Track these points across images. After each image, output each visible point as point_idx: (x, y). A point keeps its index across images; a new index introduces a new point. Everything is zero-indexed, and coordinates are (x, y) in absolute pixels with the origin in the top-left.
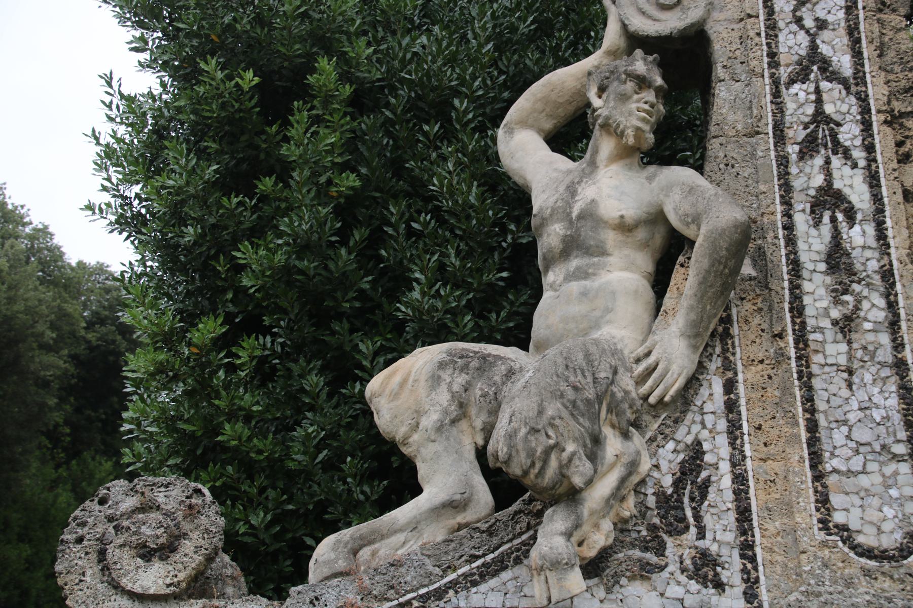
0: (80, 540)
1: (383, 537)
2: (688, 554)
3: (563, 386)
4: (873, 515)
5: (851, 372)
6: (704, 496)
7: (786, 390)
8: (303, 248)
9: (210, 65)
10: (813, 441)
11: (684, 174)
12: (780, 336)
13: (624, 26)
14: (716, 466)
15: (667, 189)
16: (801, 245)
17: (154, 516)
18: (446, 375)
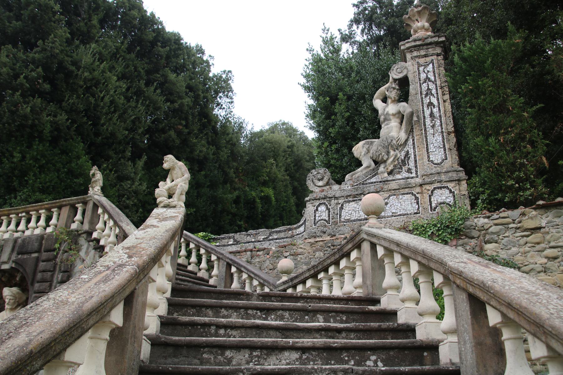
3: (382, 144)
4: (437, 158)
7: (423, 139)
8: (341, 127)
9: (321, 98)
10: (427, 147)
11: (404, 104)
12: (422, 130)
15: (400, 107)
16: (425, 113)
17: (319, 174)
18: (365, 146)
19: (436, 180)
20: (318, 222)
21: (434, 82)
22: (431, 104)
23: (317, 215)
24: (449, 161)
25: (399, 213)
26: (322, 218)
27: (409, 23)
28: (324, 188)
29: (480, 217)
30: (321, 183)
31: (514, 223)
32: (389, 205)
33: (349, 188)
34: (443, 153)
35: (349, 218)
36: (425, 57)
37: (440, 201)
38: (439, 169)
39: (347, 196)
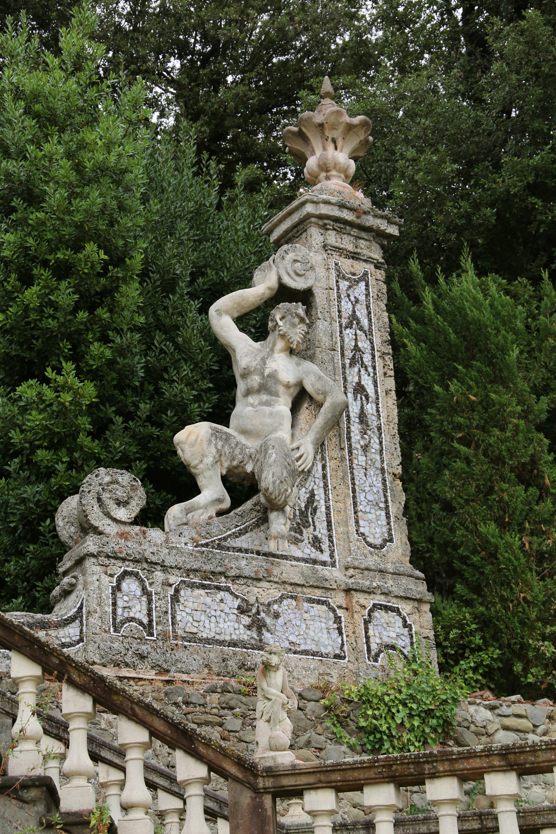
0: (89, 492)
1: (195, 510)
2: (311, 536)
4: (373, 531)
5: (366, 469)
6: (315, 513)
10: (354, 497)
13: (280, 279)
14: (318, 501)
19: (379, 587)
20: (123, 623)
21: (369, 334)
22: (360, 389)
23: (120, 603)
24: (397, 547)
25: (303, 647)
26: (132, 615)
27: (309, 135)
28: (127, 529)
29: (478, 704)
30: (122, 514)
31: (534, 732)
32: (281, 620)
33: (190, 547)
34: (384, 523)
35: (194, 630)
36: (353, 258)
37: (386, 640)
38: (372, 561)
39: (188, 572)
